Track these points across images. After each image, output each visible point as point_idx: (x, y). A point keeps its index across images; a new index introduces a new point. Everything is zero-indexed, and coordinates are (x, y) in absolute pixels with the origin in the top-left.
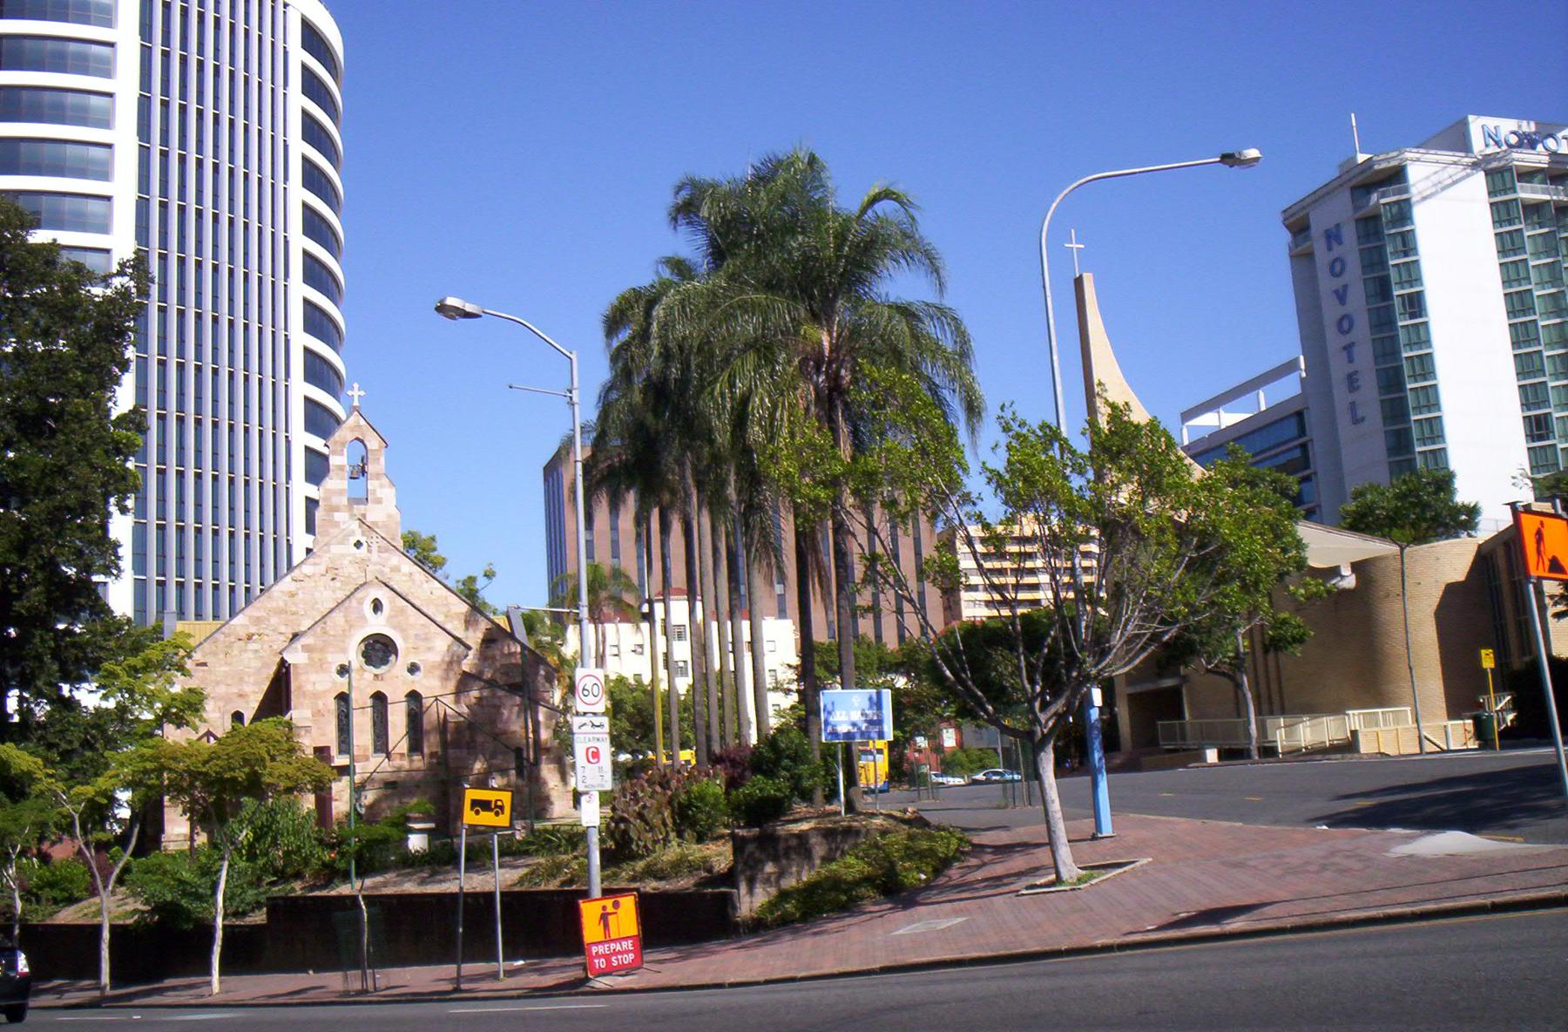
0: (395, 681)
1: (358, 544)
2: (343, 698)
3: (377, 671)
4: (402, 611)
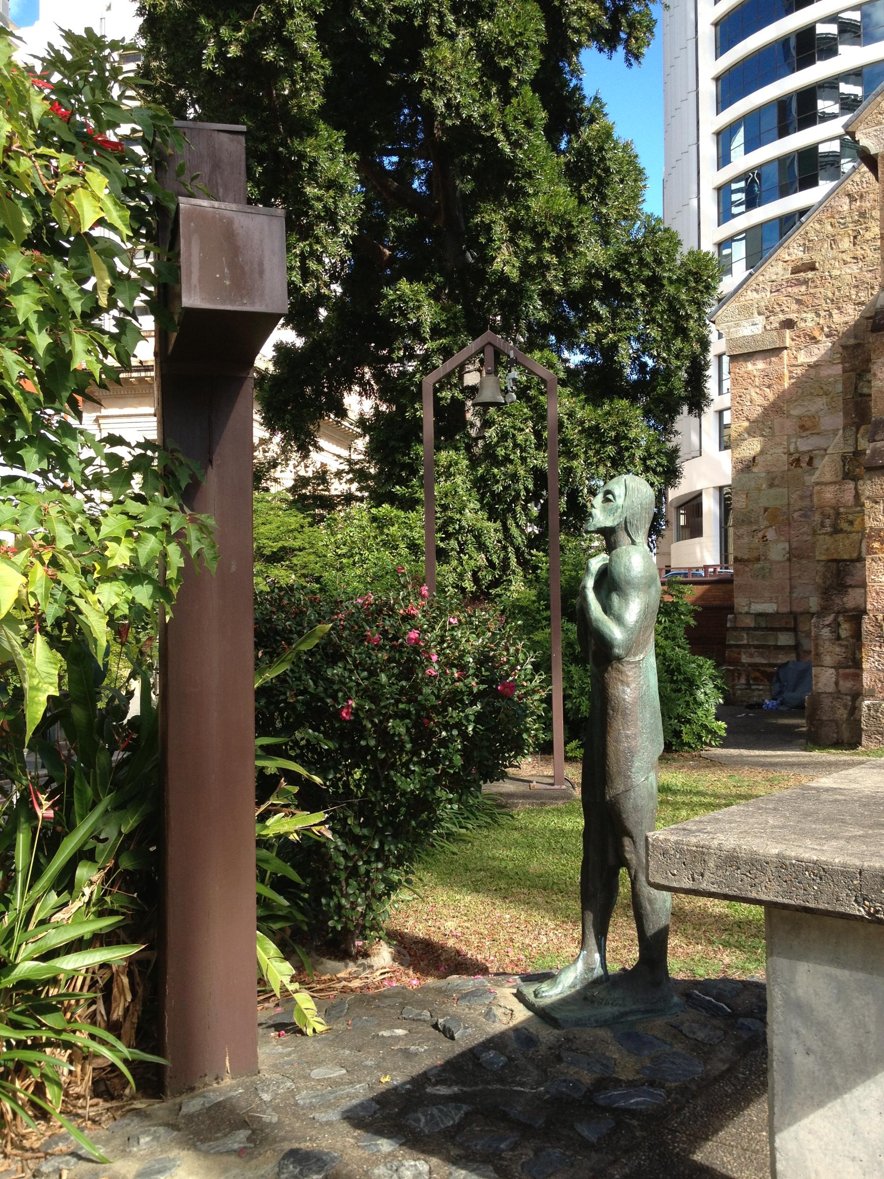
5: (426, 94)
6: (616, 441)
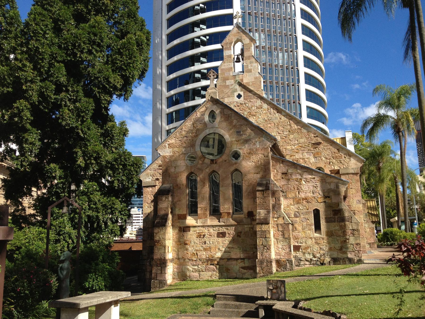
5: (60, 121)
6: (111, 209)
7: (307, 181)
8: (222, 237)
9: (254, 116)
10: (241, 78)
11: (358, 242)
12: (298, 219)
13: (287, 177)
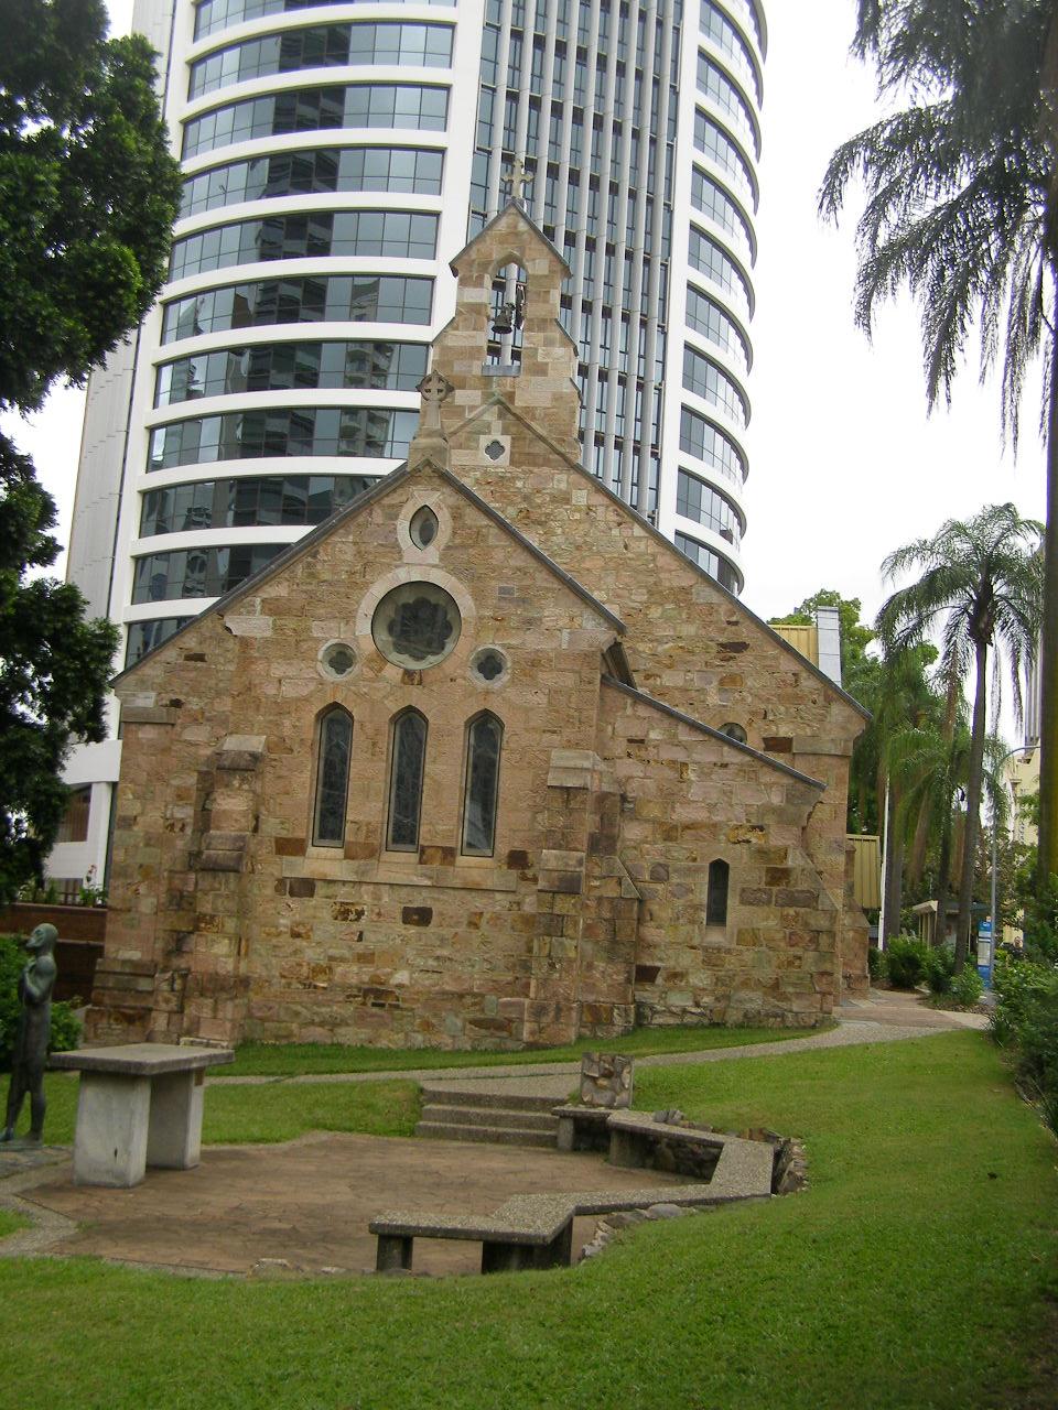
0: (449, 692)
1: (495, 449)
2: (335, 720)
3: (413, 665)
4: (479, 535)
7: (704, 774)
8: (418, 923)
9: (540, 523)
10: (509, 389)
11: (827, 967)
12: (660, 887)
13: (643, 753)
